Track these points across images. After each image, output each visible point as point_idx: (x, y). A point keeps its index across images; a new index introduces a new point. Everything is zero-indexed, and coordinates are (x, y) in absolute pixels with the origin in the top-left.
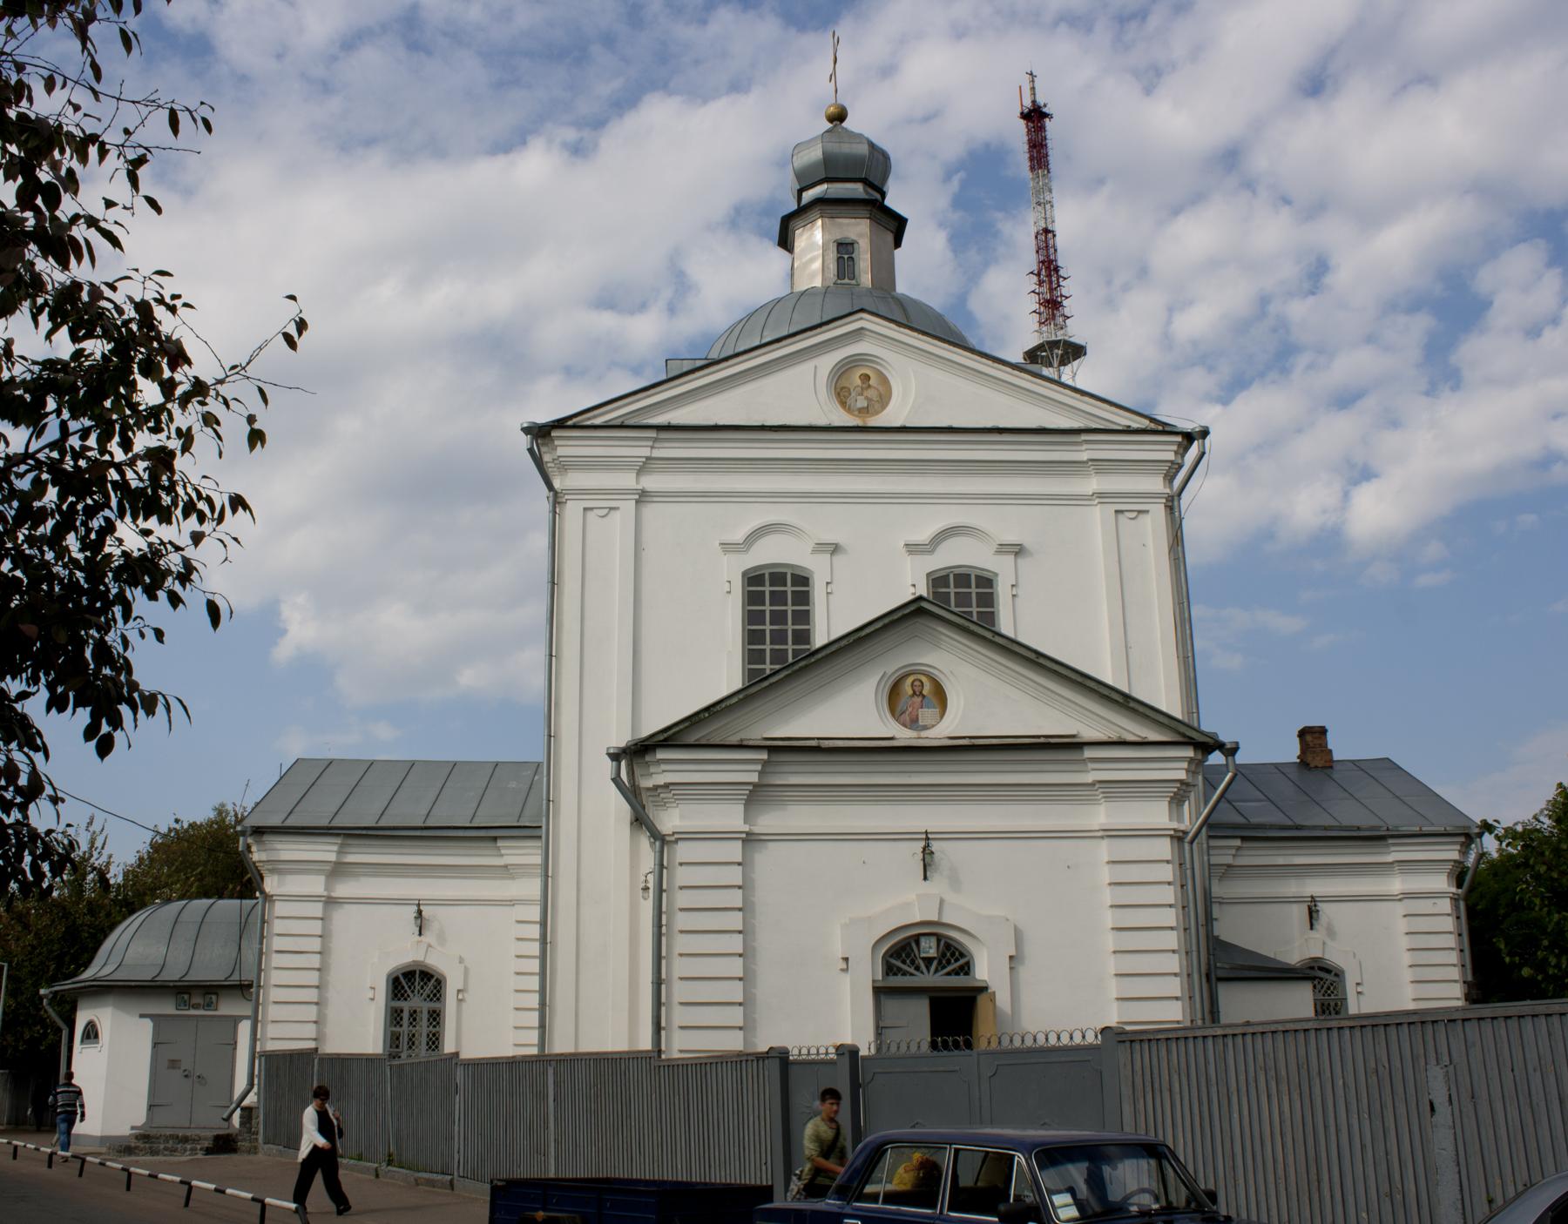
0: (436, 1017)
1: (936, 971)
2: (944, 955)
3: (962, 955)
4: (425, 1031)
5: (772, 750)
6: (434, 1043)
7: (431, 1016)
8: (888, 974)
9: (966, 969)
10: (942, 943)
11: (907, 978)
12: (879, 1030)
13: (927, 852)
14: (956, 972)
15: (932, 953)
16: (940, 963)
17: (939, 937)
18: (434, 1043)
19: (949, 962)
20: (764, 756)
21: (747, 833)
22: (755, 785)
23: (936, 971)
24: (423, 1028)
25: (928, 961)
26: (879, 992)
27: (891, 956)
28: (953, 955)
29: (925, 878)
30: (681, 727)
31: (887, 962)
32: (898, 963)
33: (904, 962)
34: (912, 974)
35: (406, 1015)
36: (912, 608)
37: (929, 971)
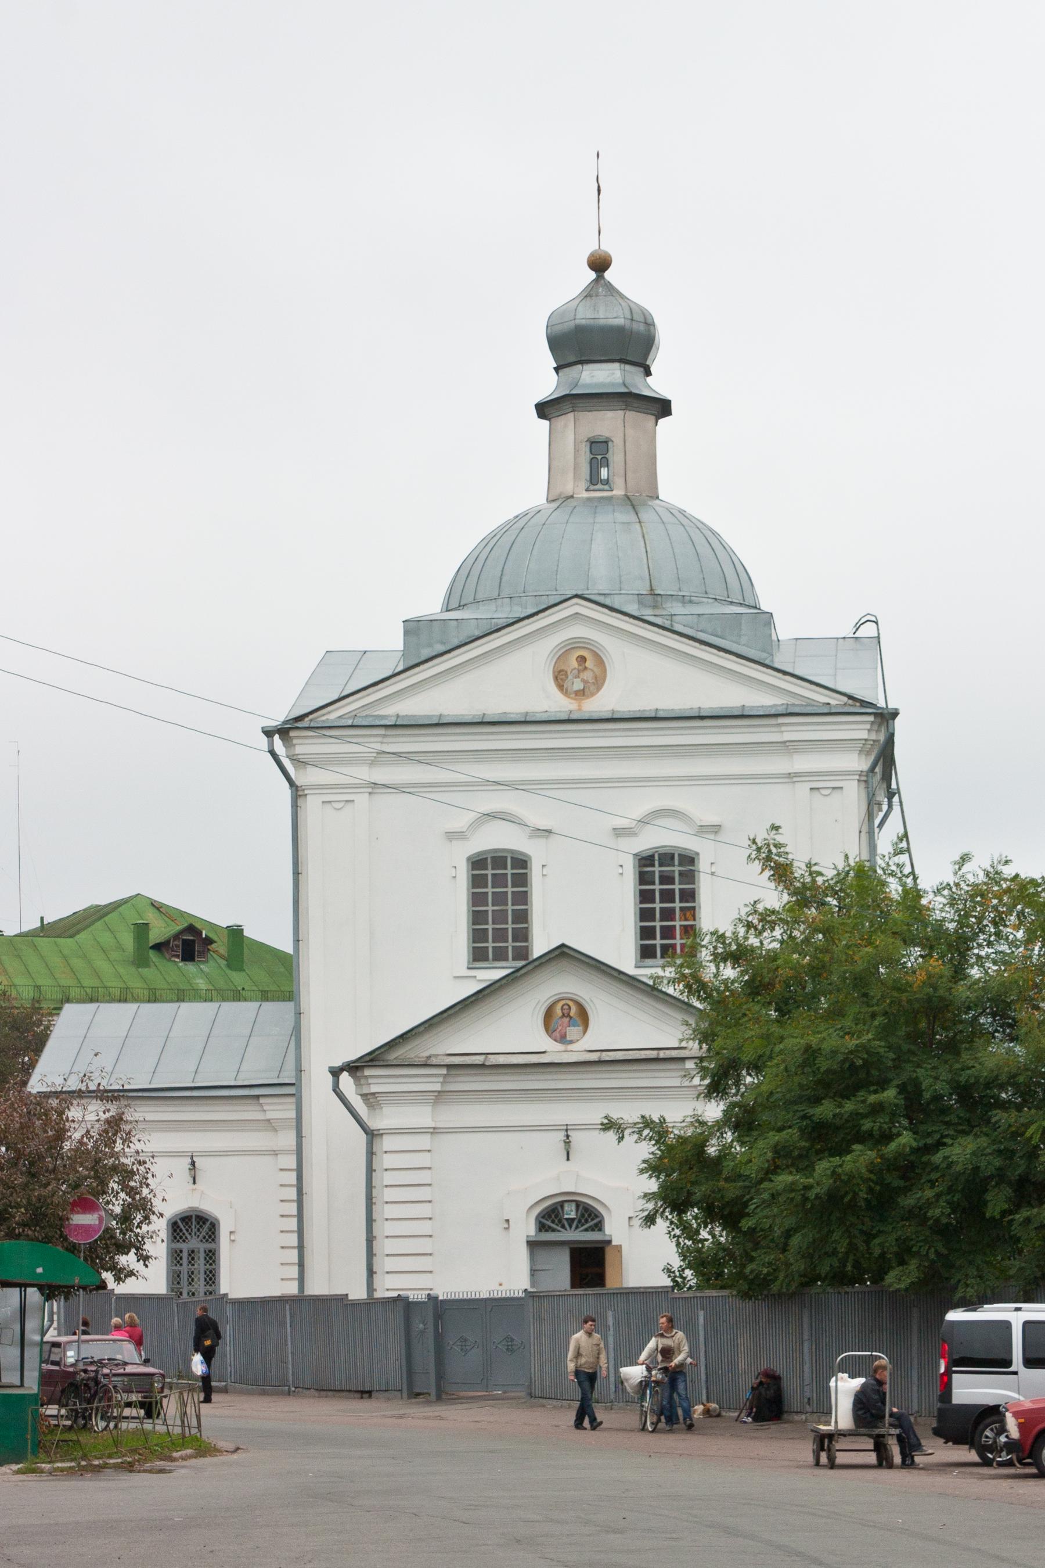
0: (212, 1256)
1: (577, 1227)
2: (583, 1216)
3: (597, 1216)
4: (202, 1269)
5: (449, 1067)
6: (211, 1279)
7: (207, 1255)
8: (540, 1230)
9: (599, 1227)
10: (581, 1208)
11: (557, 1234)
12: (533, 1272)
13: (567, 1142)
14: (591, 1229)
15: (573, 1215)
16: (580, 1221)
17: (578, 1204)
18: (211, 1279)
19: (586, 1221)
20: (444, 1071)
21: (434, 1128)
22: (439, 1092)
23: (577, 1227)
24: (200, 1265)
25: (571, 1221)
26: (533, 1245)
27: (543, 1217)
28: (590, 1215)
29: (568, 1159)
30: (382, 1050)
31: (540, 1222)
32: (549, 1223)
33: (553, 1222)
34: (559, 1231)
35: (185, 1255)
36: (557, 953)
37: (570, 1227)
